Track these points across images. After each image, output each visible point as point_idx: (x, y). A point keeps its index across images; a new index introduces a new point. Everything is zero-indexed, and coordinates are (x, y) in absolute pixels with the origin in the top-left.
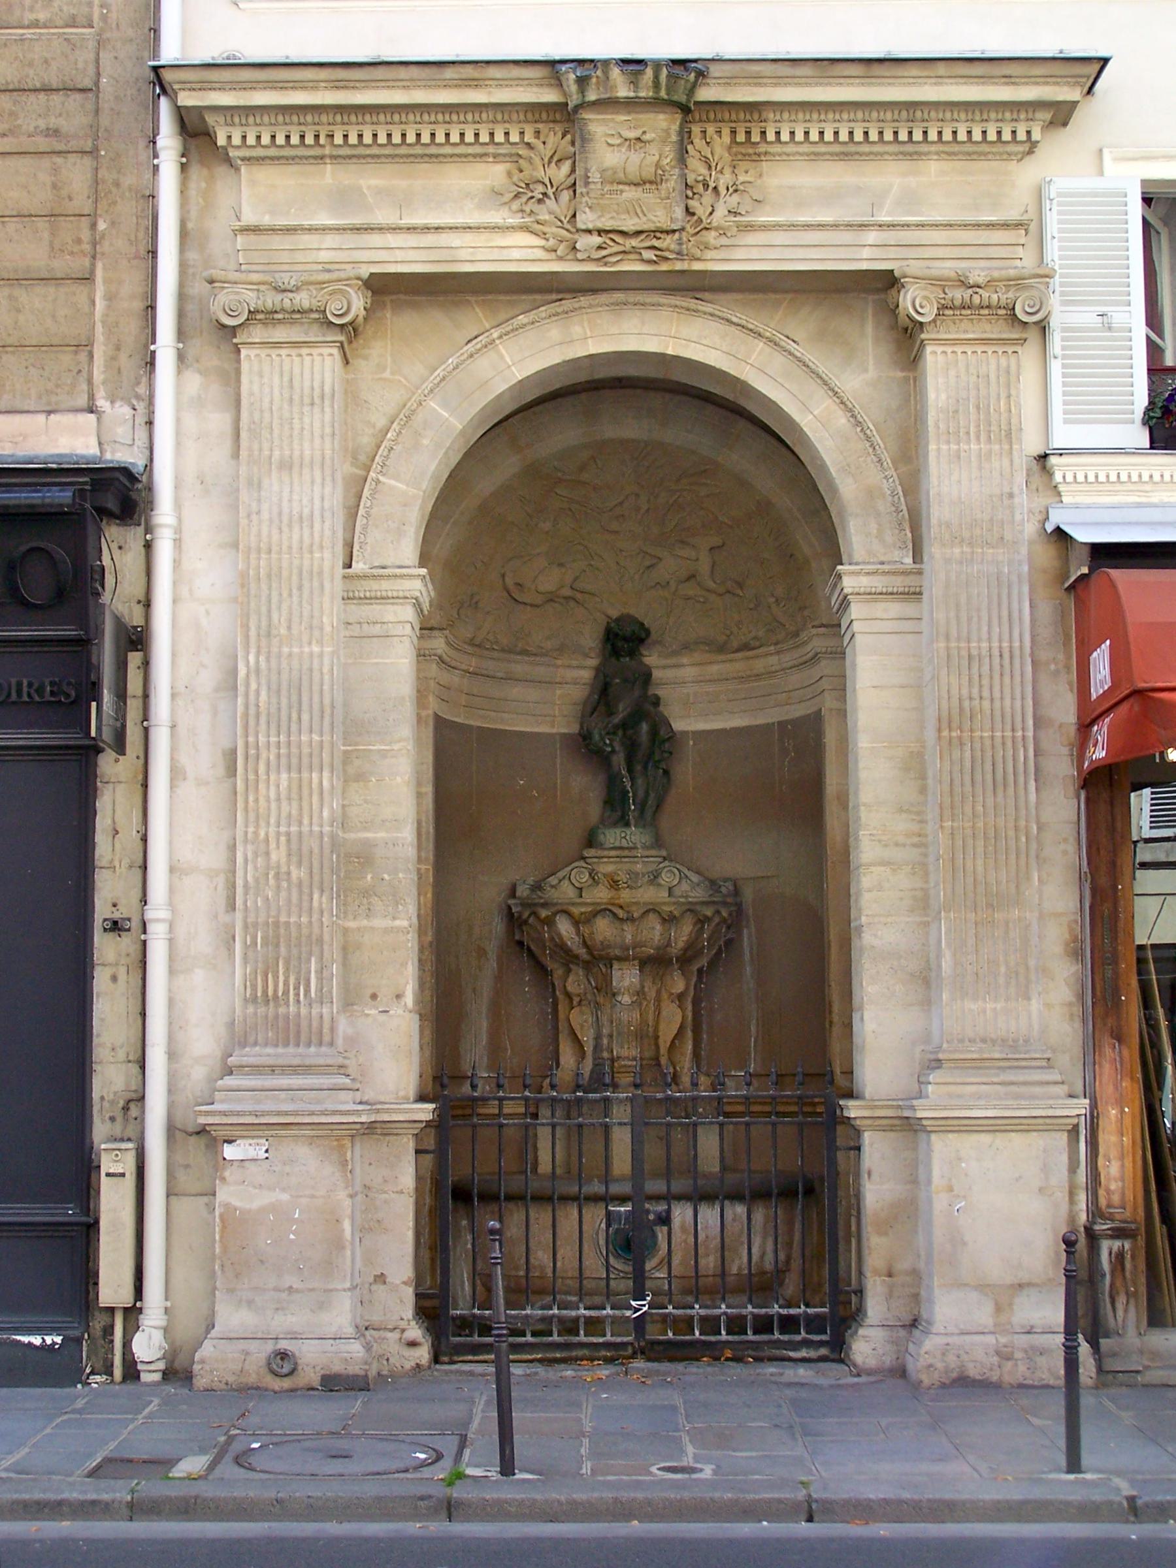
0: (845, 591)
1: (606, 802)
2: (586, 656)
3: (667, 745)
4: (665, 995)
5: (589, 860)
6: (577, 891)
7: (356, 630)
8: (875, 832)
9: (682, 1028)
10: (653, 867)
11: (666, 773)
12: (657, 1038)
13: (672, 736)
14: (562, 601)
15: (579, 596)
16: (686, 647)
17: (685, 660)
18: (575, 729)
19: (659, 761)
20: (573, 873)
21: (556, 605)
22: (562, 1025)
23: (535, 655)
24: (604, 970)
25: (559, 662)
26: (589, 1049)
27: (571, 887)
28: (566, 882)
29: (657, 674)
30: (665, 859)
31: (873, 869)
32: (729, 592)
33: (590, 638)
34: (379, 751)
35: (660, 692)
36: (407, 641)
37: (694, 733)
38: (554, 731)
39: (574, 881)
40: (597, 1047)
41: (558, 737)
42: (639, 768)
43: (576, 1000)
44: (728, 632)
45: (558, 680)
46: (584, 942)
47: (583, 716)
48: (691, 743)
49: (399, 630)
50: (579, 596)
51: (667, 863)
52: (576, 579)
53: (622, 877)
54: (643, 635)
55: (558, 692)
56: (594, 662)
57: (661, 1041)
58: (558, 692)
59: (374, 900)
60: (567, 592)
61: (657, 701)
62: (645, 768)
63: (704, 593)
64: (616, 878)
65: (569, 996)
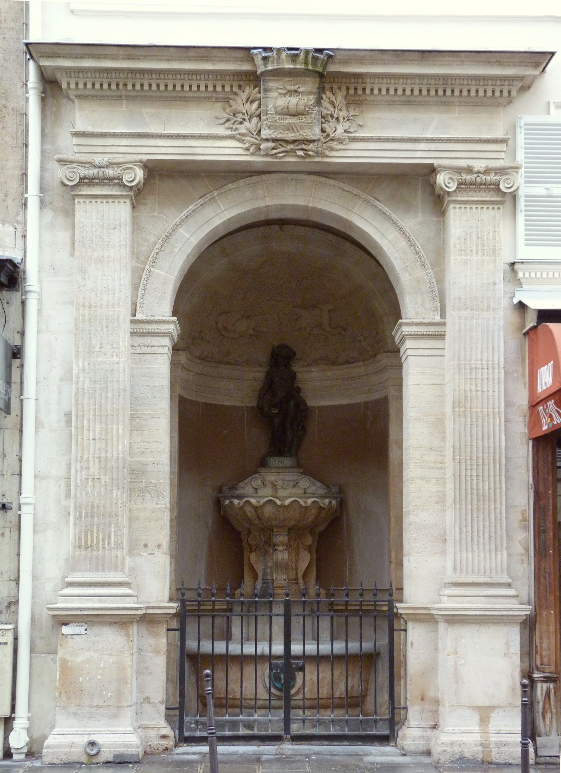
0: (403, 333)
2: (261, 366)
4: (301, 546)
5: (261, 474)
6: (254, 491)
7: (138, 350)
8: (417, 461)
9: (310, 563)
10: (295, 478)
11: (303, 428)
12: (297, 569)
13: (307, 408)
16: (315, 362)
17: (314, 369)
18: (254, 404)
22: (246, 562)
23: (233, 365)
24: (269, 532)
25: (246, 369)
26: (260, 575)
27: (251, 488)
28: (249, 485)
29: (299, 376)
30: (302, 473)
31: (416, 481)
33: (263, 357)
34: (150, 414)
35: (300, 385)
36: (165, 357)
38: (244, 405)
39: (253, 484)
40: (265, 574)
43: (254, 548)
46: (259, 517)
49: (161, 350)
51: (303, 476)
53: (280, 483)
56: (266, 369)
57: (299, 570)
58: (246, 385)
59: (146, 494)
60: (251, 332)
61: (299, 390)
64: (276, 483)
65: (249, 545)
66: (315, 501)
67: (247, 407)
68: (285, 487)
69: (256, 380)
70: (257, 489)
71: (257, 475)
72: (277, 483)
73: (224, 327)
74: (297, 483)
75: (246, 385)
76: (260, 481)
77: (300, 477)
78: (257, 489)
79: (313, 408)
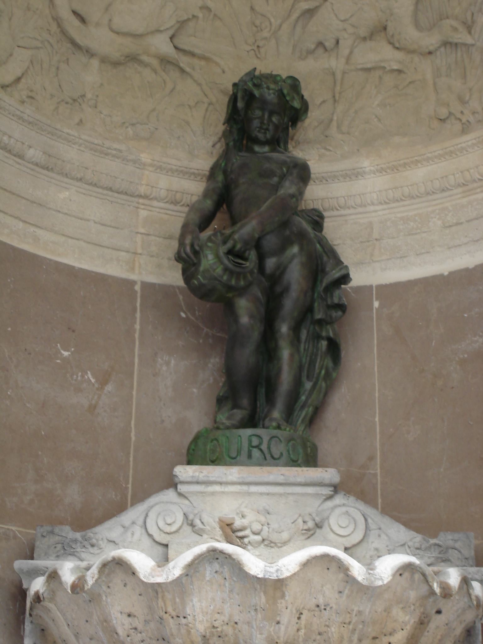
1: (220, 401)
3: (337, 293)
14: (155, 62)
15: (184, 61)
17: (366, 164)
19: (320, 322)
20: (152, 515)
21: (147, 72)
27: (147, 541)
28: (138, 531)
30: (336, 488)
32: (446, 44)
37: (381, 287)
38: (133, 277)
39: (153, 530)
41: (138, 288)
42: (284, 329)
44: (443, 112)
45: (142, 190)
47: (185, 227)
48: (376, 304)
50: (184, 61)
51: (339, 499)
52: (182, 24)
54: (296, 104)
55: (143, 213)
62: (296, 329)
63: (399, 55)
64: (238, 523)
66: (408, 567)
67: (145, 286)
68: (274, 537)
69: (175, 202)
70: (167, 546)
71: (170, 494)
72: (245, 522)
73: (75, 12)
74: (318, 526)
75: (143, 213)
76: (180, 518)
77: (329, 504)
78: (167, 546)
79: (366, 290)
